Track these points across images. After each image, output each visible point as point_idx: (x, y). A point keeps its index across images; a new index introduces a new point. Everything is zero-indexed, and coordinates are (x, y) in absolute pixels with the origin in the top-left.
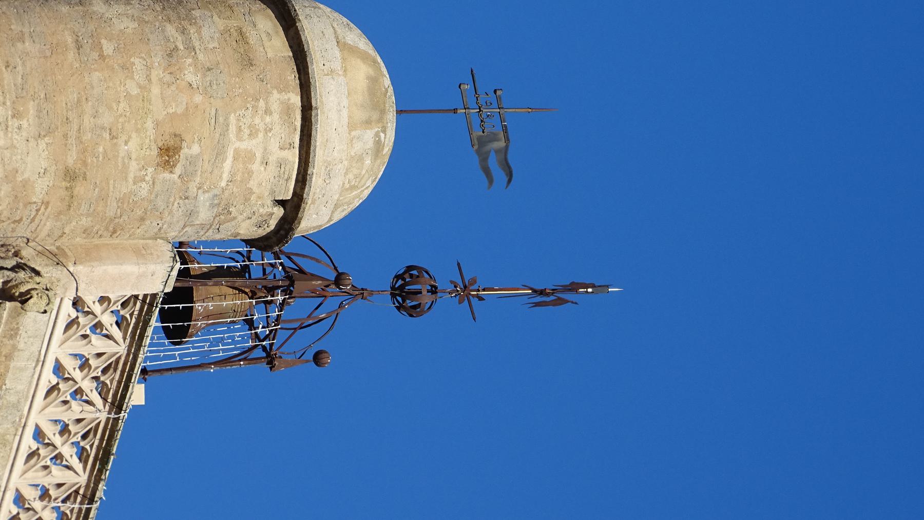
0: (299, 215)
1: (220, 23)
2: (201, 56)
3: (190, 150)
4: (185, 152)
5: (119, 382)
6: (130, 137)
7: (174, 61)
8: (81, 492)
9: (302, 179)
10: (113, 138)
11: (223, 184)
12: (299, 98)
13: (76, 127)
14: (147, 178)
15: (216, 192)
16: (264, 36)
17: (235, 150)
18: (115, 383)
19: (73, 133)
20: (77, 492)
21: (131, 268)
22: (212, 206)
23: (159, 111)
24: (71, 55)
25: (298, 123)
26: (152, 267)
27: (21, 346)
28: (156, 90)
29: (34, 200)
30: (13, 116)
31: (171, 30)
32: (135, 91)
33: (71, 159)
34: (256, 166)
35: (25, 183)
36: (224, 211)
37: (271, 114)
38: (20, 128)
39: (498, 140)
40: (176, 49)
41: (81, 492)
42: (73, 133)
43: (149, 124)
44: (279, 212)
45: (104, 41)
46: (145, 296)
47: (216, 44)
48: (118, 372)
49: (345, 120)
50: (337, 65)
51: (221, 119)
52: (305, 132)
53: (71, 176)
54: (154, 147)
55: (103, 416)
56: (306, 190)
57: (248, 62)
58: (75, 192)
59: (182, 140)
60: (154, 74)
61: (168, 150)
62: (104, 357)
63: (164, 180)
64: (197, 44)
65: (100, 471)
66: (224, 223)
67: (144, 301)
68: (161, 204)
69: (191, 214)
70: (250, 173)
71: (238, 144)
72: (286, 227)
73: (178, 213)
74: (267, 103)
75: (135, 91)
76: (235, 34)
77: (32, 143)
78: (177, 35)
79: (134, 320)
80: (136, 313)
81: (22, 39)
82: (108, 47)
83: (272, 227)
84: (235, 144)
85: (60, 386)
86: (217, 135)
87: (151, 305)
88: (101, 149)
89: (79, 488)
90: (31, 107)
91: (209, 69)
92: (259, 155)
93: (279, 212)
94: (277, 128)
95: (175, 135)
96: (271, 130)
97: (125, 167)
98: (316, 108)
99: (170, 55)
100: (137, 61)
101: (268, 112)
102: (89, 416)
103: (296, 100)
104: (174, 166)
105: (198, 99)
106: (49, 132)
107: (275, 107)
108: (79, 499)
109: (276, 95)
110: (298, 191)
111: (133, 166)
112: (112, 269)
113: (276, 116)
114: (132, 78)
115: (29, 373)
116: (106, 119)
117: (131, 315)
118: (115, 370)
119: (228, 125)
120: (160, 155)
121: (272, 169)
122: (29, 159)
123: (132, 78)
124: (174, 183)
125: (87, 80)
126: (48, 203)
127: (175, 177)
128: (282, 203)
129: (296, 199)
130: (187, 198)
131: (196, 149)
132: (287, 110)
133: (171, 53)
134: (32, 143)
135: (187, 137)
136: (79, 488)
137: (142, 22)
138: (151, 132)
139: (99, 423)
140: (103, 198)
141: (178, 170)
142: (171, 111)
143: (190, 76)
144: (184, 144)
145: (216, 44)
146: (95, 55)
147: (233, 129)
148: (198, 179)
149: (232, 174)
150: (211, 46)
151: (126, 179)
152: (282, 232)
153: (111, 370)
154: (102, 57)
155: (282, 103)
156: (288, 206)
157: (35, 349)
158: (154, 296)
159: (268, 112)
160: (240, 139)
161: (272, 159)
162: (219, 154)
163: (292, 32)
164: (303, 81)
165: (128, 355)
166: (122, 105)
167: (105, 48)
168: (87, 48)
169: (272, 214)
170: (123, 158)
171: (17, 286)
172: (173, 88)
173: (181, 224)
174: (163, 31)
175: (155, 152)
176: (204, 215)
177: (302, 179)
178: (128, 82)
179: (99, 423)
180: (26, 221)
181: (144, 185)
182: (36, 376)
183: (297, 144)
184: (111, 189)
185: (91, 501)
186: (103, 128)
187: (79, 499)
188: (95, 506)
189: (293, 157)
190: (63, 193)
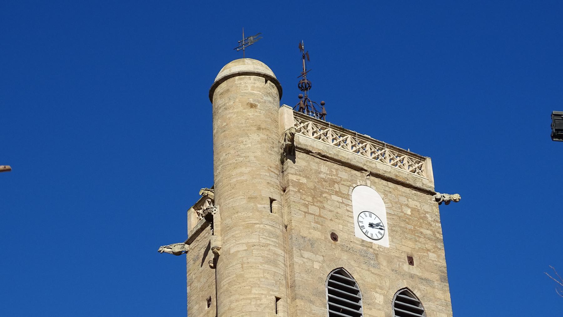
0: (269, 75)
1: (219, 100)
2: (226, 102)
3: (251, 101)
4: (252, 102)
5: (320, 124)
6: (248, 115)
8: (353, 137)
9: (258, 74)
10: (248, 119)
11: (261, 93)
12: (237, 77)
13: (246, 128)
14: (260, 111)
15: (263, 95)
16: (221, 89)
17: (251, 90)
18: (321, 125)
19: (247, 128)
20: (353, 138)
21: (286, 116)
22: (267, 96)
23: (241, 109)
24: (227, 132)
25: (244, 76)
26: (285, 111)
27: (310, 144)
28: (235, 110)
29: (266, 137)
30: (243, 143)
31: (220, 111)
32: (236, 115)
33: (254, 129)
34: (256, 85)
35: (262, 140)
36: (269, 94)
37: (241, 83)
38: (246, 141)
39: (251, 39)
41: (353, 137)
42: (247, 128)
43: (244, 111)
44: (269, 82)
45: (223, 126)
46: (294, 115)
47: (223, 99)
48: (317, 124)
49: (243, 66)
50: (228, 70)
51: (243, 94)
52: (246, 74)
53: (259, 129)
54: (251, 109)
55: (331, 129)
56: (261, 73)
57: (228, 90)
58: (264, 128)
59: (249, 103)
60: (231, 112)
61: (251, 106)
62: (313, 127)
63: (260, 107)
64: (223, 104)
65: (346, 131)
66: (272, 95)
67: (296, 115)
68: (267, 108)
69: (270, 102)
70: (257, 87)
71: (249, 90)
72: (273, 80)
73: (270, 105)
74: (238, 84)
75: (236, 115)
76: (221, 96)
77: (250, 138)
78: (221, 109)
79: (302, 119)
80: (300, 118)
81: (223, 145)
82: (225, 124)
83: (274, 85)
84: (250, 90)
85: (322, 138)
86: (247, 95)
87: (297, 113)
88: (251, 122)
89: (352, 137)
90: (240, 139)
91: (230, 99)
92: (252, 85)
93: (269, 82)
94: (245, 81)
95: (247, 104)
96: (245, 82)
97: (256, 116)
98: (239, 71)
99: (226, 109)
100: (228, 116)
101: (241, 84)
102: (331, 133)
103: (237, 77)
104: (256, 104)
105: (237, 100)
106: (247, 134)
107: (239, 82)
108: (355, 137)
109: (236, 82)
110: (262, 76)
111: (256, 114)
112: (286, 120)
113: (242, 82)
114: (232, 117)
115: (318, 144)
116: (243, 121)
117: (301, 119)
118: (317, 125)
119: (244, 92)
120: (253, 108)
121: (256, 82)
122: (255, 139)
123: (232, 117)
124: (261, 105)
125: (233, 127)
126: (267, 135)
127: (259, 104)
128: (266, 82)
129: (265, 77)
130: (265, 102)
131: (251, 100)
132: (241, 79)
133: (226, 109)
134: (250, 138)
135: (248, 102)
136: (352, 137)
137: (218, 119)
138: (247, 110)
139: (333, 130)
140: (266, 122)
141: (257, 104)
142: (241, 106)
143: (231, 103)
144: (250, 102)
145: (223, 99)
146: (226, 127)
147: (245, 91)
148: (260, 99)
149: (258, 91)
150: (224, 100)
151: (260, 116)
152: (275, 82)
153: (317, 126)
155: (238, 81)
156: (267, 79)
157: (310, 141)
158: (294, 112)
159: (241, 84)
160: (248, 89)
161: (253, 82)
162: (252, 94)
163: (220, 82)
164: (232, 76)
165: (312, 121)
166: (239, 118)
167: (225, 125)
168: (225, 129)
169: (269, 83)
170: (254, 116)
171: (289, 137)
172: (234, 107)
173: (273, 105)
174: (220, 113)
175: (252, 109)
176: (270, 99)
177: (258, 74)
178: (233, 117)
179: (333, 130)
180: (273, 141)
181: (261, 112)
182: (318, 142)
183: (249, 76)
184: (263, 119)
185: (355, 134)
186: (246, 121)
187: (355, 137)
188: (357, 133)
189: (253, 77)
190: (264, 130)
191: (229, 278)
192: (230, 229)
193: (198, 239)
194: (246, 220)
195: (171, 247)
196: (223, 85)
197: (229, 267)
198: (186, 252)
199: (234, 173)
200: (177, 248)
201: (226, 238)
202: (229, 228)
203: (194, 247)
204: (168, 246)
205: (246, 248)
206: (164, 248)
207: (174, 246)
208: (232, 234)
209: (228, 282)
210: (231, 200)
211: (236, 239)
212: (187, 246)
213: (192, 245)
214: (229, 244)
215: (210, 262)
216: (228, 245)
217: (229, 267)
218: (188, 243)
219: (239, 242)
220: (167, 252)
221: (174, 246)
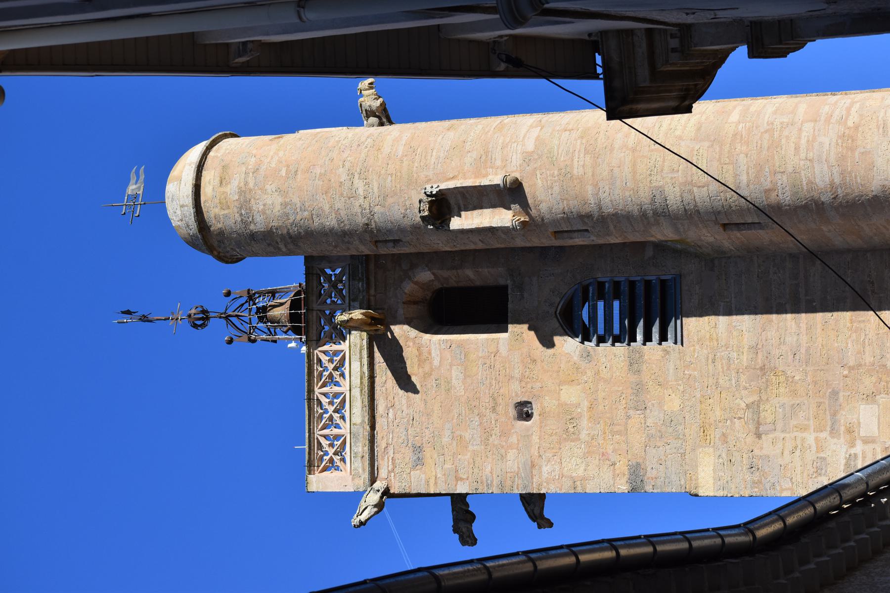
7: (257, 167)
40: (253, 173)
57: (225, 168)
103: (212, 154)
154: (288, 166)
191: (577, 152)
192: (487, 153)
193: (383, 445)
194: (487, 130)
195: (364, 507)
196: (208, 176)
197: (556, 154)
198: (386, 493)
199: (386, 150)
200: (373, 498)
201: (498, 163)
202: (484, 157)
203: (390, 463)
204: (358, 512)
205: (540, 128)
206: (357, 517)
207: (365, 502)
208: (499, 148)
209: (582, 155)
210: (434, 154)
211: (513, 141)
212: (377, 486)
213: (383, 473)
214: (514, 154)
215: (514, 221)
216: (514, 157)
217: (556, 154)
218: (373, 480)
219: (521, 138)
220: (368, 517)
221: (365, 502)
